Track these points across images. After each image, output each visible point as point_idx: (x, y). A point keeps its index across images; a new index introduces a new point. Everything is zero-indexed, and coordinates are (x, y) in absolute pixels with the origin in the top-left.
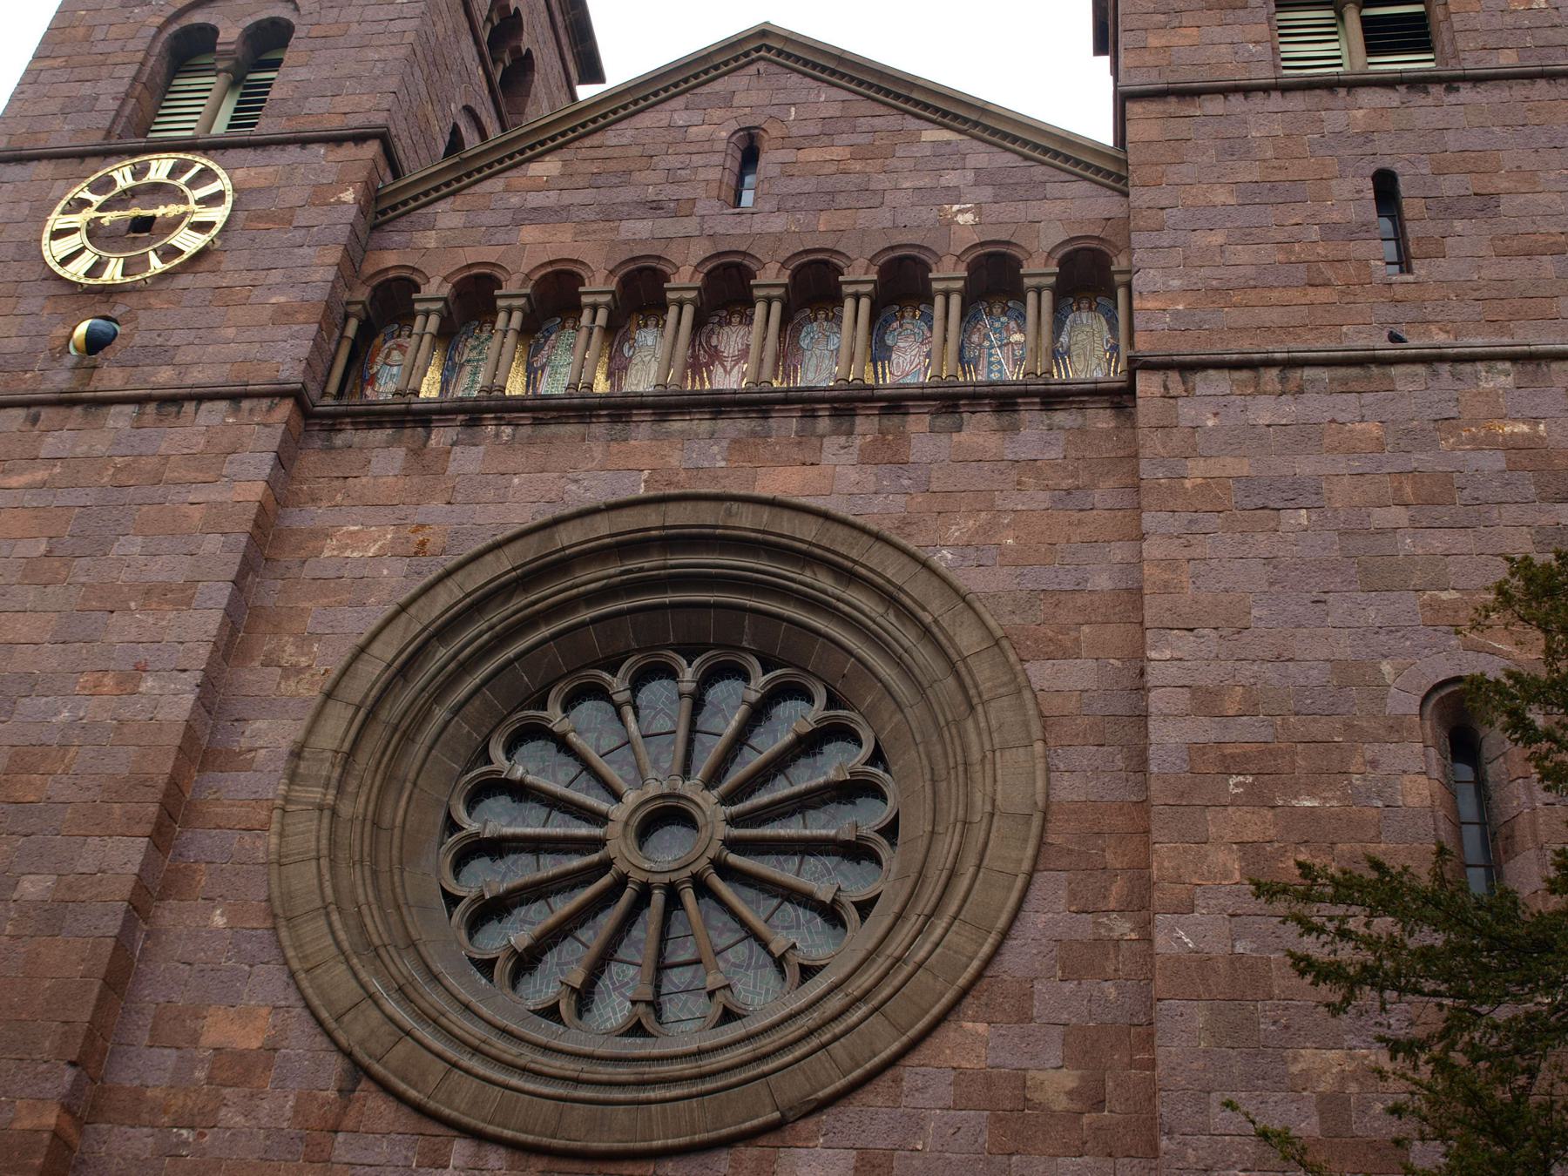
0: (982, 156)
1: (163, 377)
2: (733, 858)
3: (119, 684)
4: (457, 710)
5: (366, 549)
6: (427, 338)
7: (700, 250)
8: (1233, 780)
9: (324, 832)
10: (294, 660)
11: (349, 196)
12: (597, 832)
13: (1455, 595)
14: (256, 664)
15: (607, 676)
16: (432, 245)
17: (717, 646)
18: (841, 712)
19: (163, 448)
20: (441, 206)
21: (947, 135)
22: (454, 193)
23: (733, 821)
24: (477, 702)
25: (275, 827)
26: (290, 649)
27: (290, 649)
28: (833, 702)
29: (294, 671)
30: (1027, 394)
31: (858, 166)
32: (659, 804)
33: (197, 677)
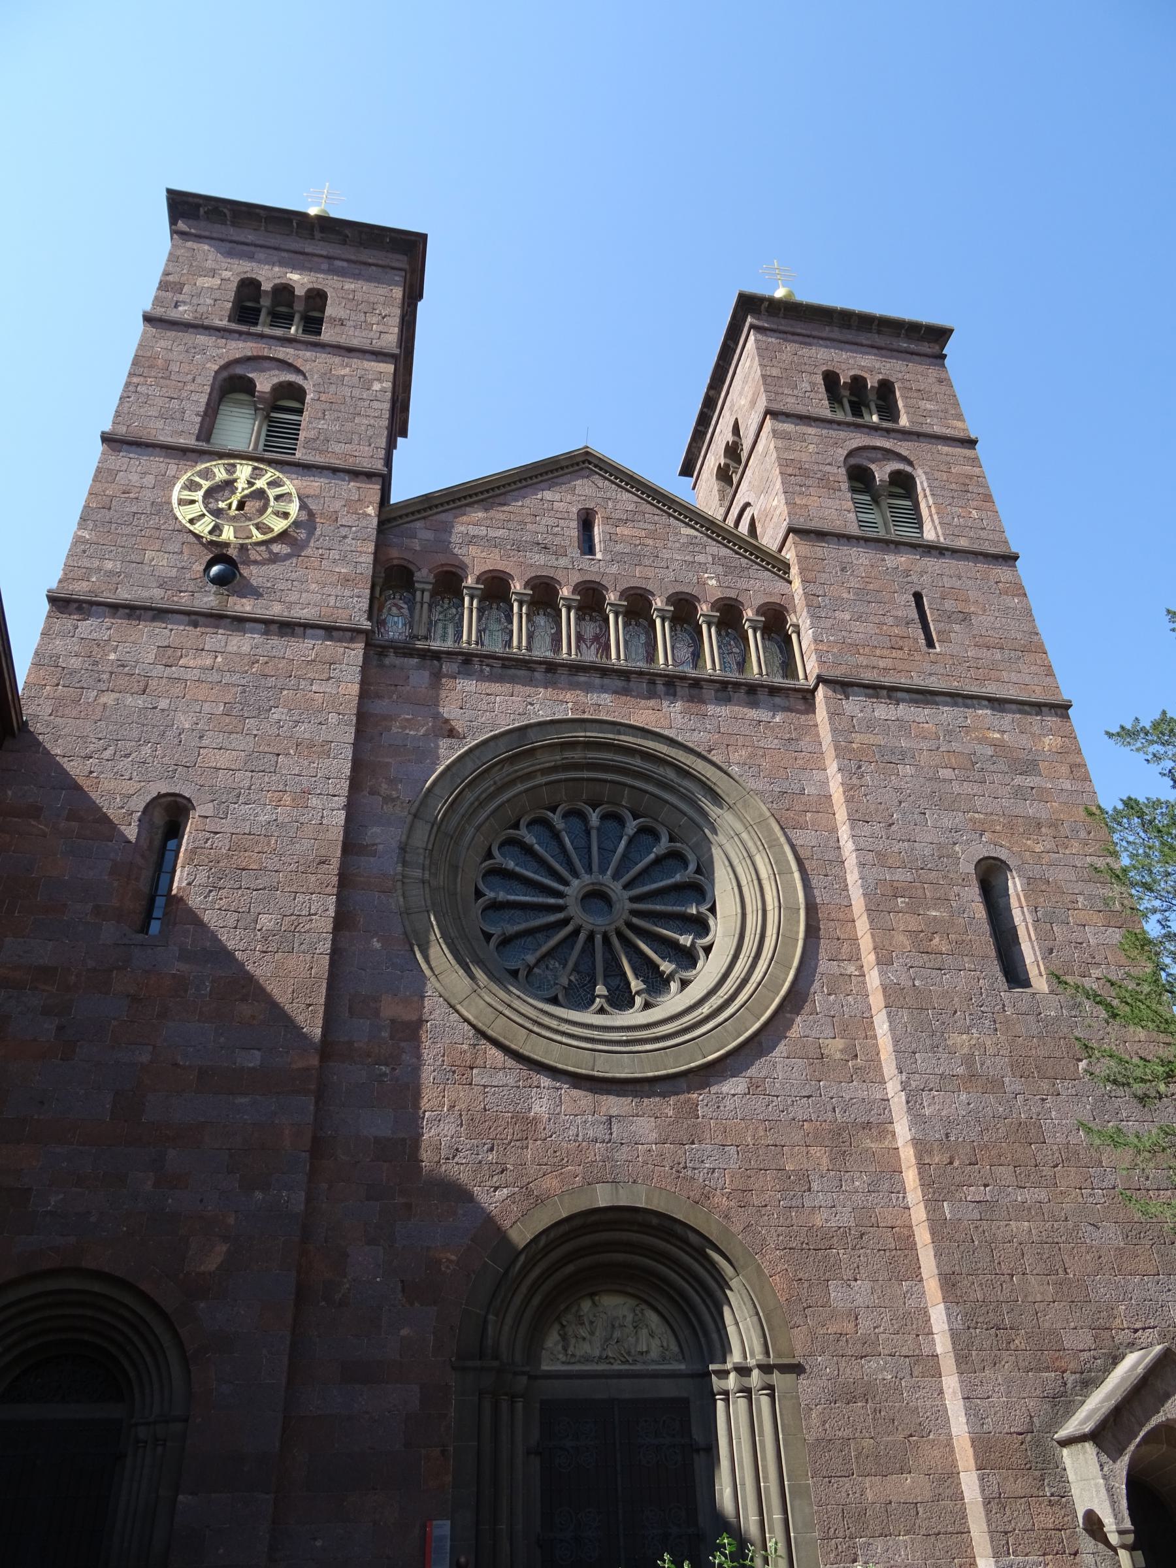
0: (714, 548)
1: (276, 610)
2: (635, 920)
3: (294, 800)
4: (478, 828)
5: (417, 730)
6: (426, 606)
7: (576, 578)
8: (899, 900)
9: (428, 896)
10: (388, 792)
11: (371, 511)
12: (561, 901)
13: (982, 816)
14: (366, 793)
15: (551, 815)
16: (418, 548)
17: (608, 803)
18: (678, 844)
19: (288, 655)
20: (418, 524)
21: (696, 533)
22: (424, 518)
23: (633, 899)
24: (487, 824)
25: (400, 892)
26: (384, 786)
27: (384, 786)
28: (672, 839)
29: (388, 799)
30: (762, 686)
31: (650, 542)
32: (590, 888)
33: (342, 801)
